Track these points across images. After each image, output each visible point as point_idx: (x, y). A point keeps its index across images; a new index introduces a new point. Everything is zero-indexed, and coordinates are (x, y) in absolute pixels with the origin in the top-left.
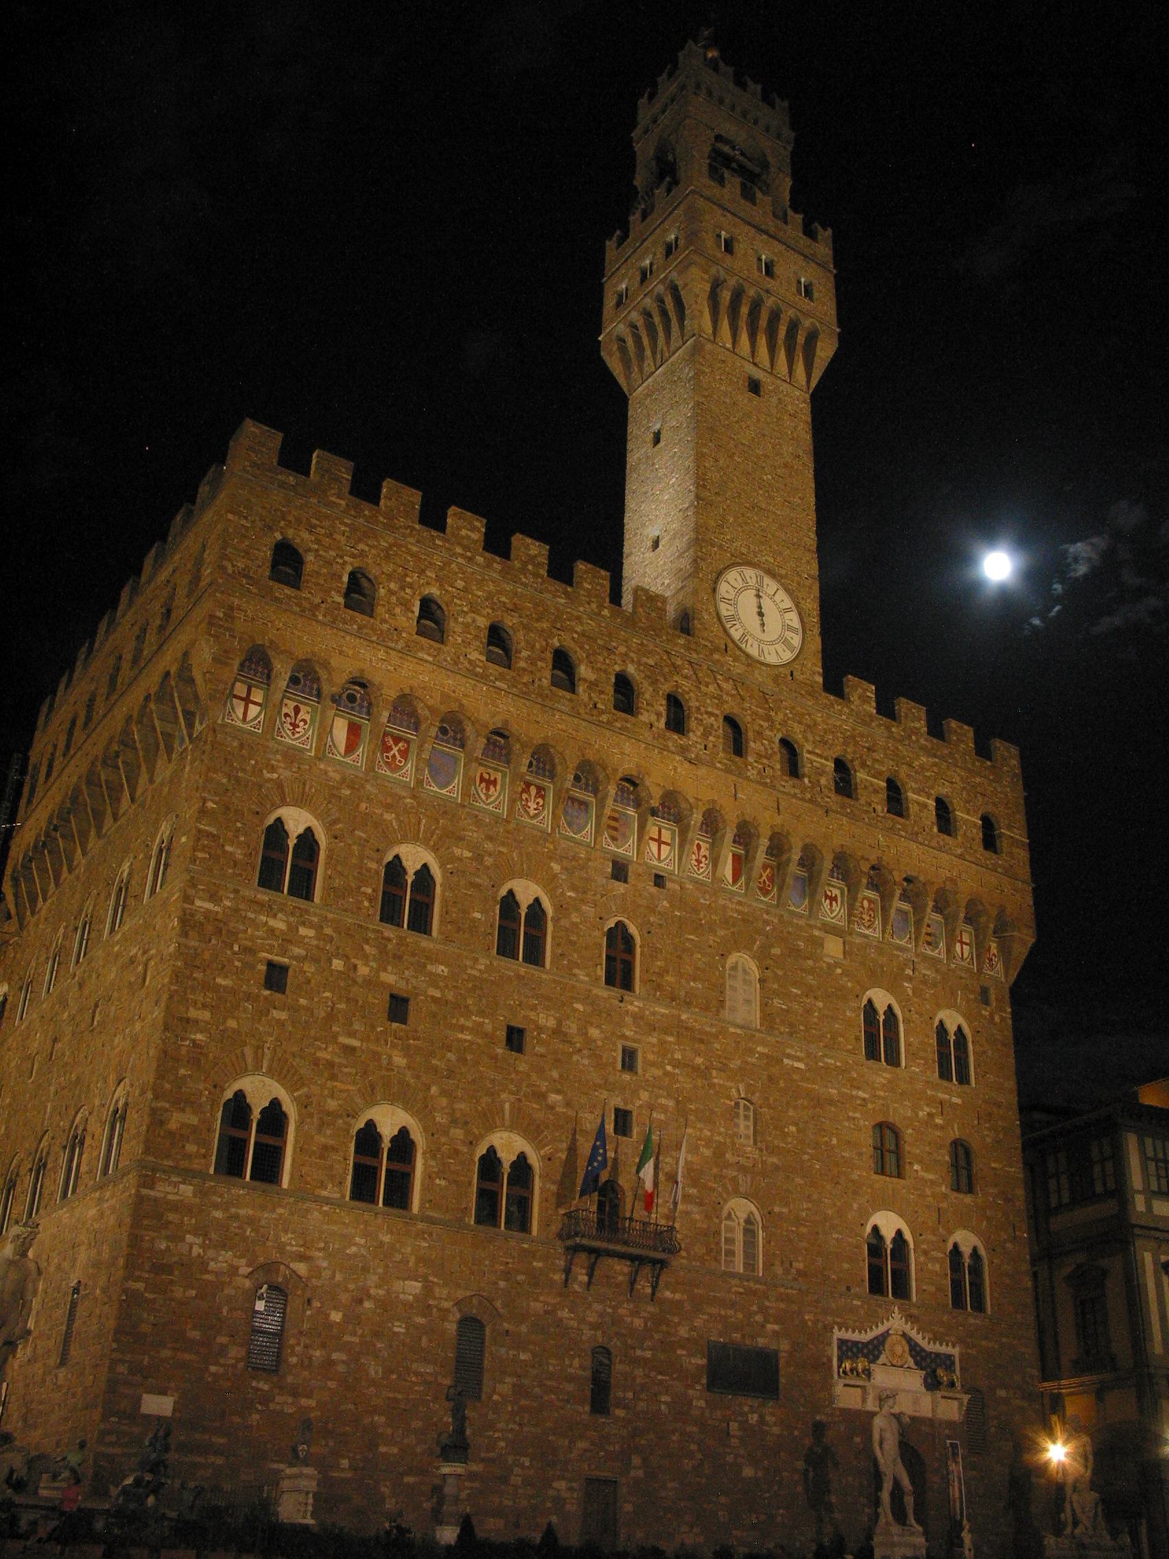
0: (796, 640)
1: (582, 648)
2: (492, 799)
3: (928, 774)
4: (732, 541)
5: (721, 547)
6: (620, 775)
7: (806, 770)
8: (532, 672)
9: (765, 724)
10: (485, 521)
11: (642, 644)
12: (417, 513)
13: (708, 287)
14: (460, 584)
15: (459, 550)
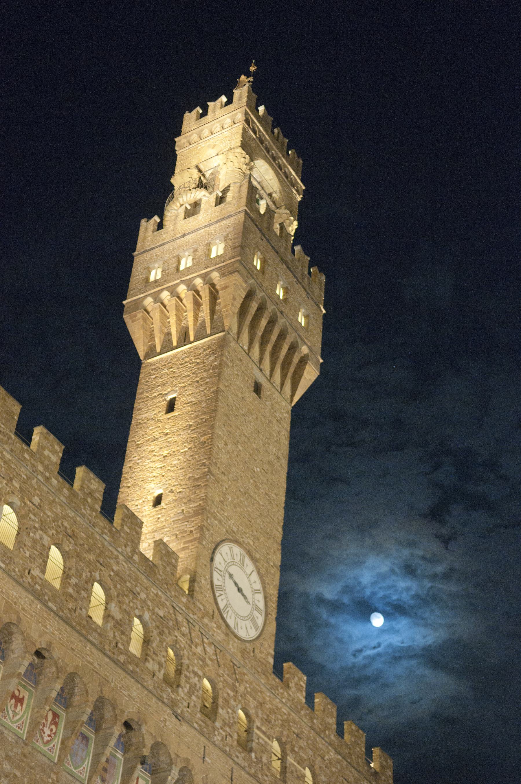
0: (260, 621)
1: (115, 587)
2: (18, 717)
3: (334, 769)
4: (228, 518)
5: (220, 521)
6: (125, 718)
7: (254, 745)
8: (76, 600)
9: (232, 694)
10: (63, 447)
11: (157, 595)
12: (15, 424)
13: (244, 294)
14: (36, 500)
15: (40, 468)
